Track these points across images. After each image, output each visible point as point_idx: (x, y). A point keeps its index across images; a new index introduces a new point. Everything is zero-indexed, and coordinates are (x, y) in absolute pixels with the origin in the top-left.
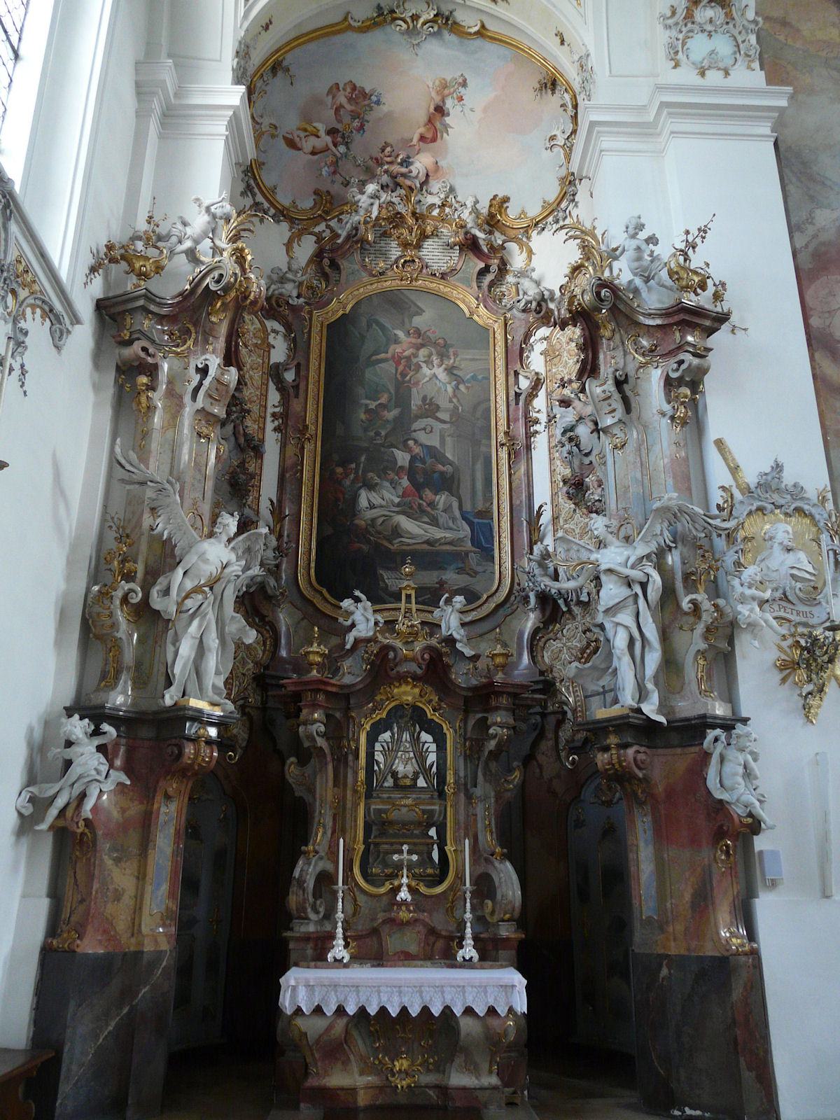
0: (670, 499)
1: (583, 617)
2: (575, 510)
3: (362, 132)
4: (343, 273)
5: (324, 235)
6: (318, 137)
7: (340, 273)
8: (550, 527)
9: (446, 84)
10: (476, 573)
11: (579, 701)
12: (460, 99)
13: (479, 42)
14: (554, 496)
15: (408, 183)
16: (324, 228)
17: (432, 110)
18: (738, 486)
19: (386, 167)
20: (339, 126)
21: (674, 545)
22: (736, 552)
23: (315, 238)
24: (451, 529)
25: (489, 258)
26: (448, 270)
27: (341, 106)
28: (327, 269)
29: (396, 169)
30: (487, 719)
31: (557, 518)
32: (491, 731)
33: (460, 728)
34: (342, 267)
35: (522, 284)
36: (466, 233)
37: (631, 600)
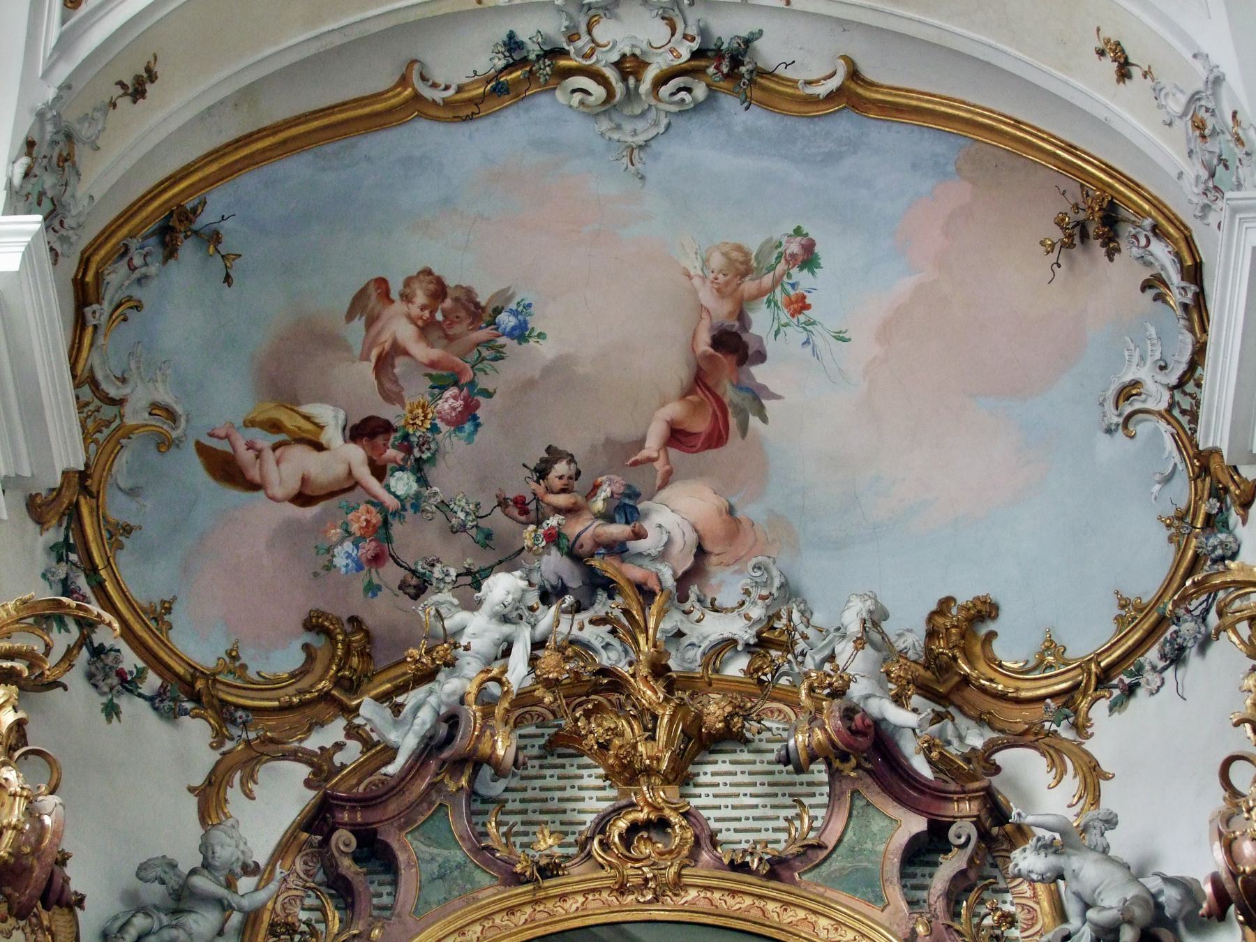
3: (468, 427)
4: (408, 878)
5: (338, 759)
6: (319, 447)
7: (395, 883)
9: (746, 262)
12: (800, 305)
13: (845, 125)
15: (635, 572)
16: (340, 737)
17: (704, 344)
20: (390, 413)
23: (304, 771)
25: (942, 796)
26: (794, 849)
27: (397, 349)
28: (347, 865)
29: (585, 529)
34: (402, 857)
35: (1075, 875)
36: (849, 713)
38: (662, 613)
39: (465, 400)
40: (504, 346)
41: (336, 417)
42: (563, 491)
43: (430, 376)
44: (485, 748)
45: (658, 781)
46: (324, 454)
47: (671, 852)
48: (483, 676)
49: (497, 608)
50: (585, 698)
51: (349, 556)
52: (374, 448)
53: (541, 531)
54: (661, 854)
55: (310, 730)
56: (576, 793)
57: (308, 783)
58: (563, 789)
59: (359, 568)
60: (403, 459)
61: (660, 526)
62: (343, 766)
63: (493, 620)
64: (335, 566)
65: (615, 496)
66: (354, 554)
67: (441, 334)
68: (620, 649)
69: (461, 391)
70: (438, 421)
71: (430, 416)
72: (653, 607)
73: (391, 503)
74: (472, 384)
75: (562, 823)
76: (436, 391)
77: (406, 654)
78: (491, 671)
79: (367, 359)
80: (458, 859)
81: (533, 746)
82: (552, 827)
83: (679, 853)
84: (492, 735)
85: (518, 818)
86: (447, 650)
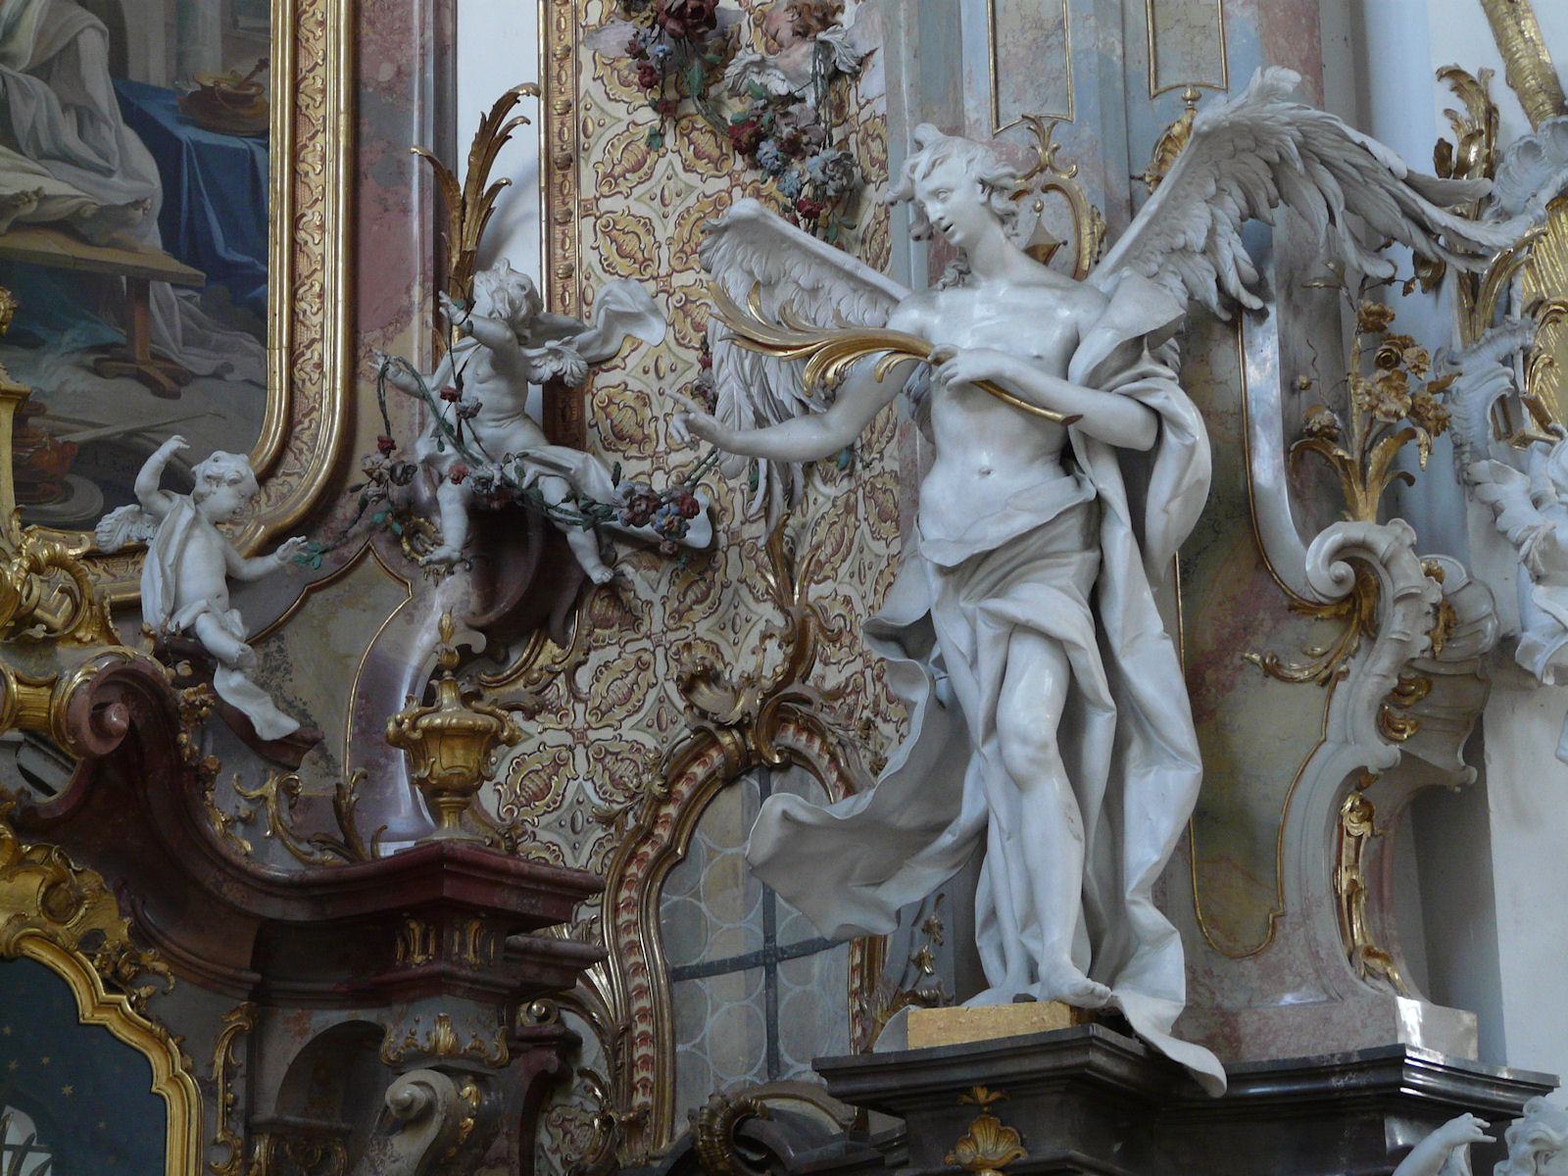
0: (1268, 93)
1: (679, 615)
2: (656, 138)
8: (531, 203)
10: (183, 378)
11: (642, 991)
14: (556, 60)
18: (1513, 80)
21: (1255, 303)
22: (1507, 360)
24: (68, 158)
30: (377, 1033)
31: (569, 162)
32: (404, 1089)
33: (229, 1073)
37: (1072, 530)
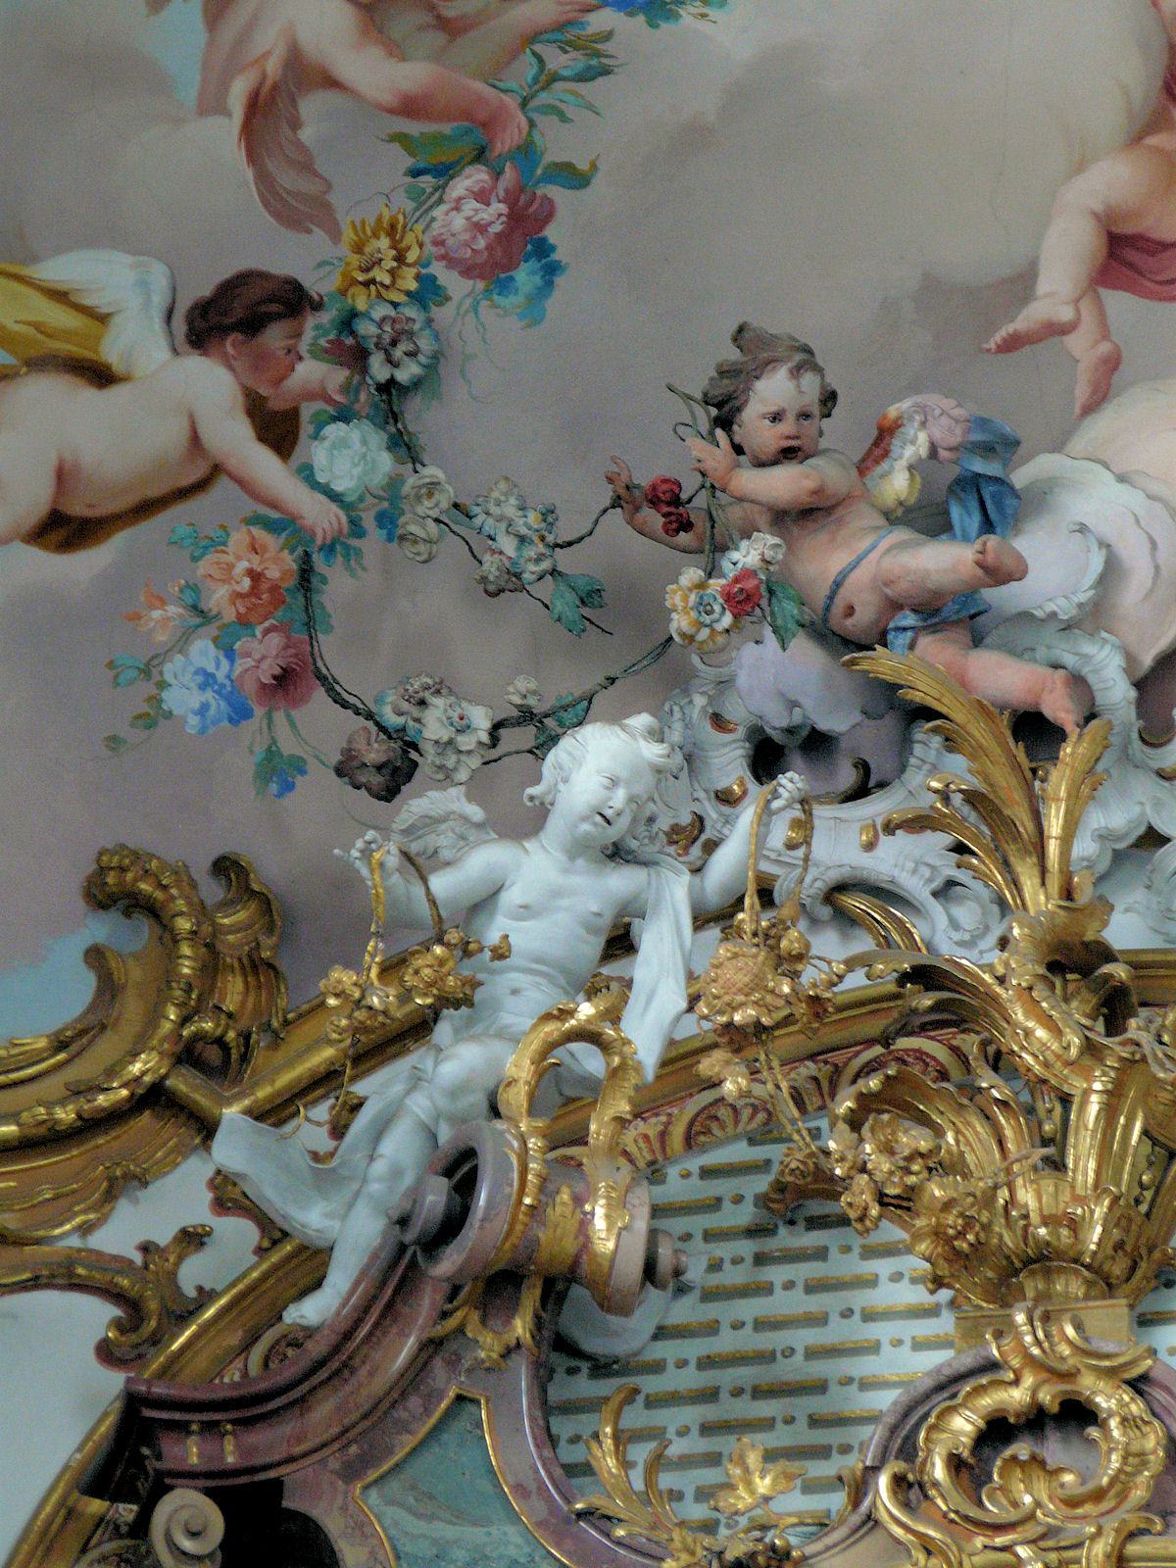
3: (525, 276)
5: (193, 1273)
6: (101, 376)
16: (198, 1210)
19: (746, 555)
23: (97, 1316)
38: (1089, 785)
39: (511, 199)
40: (608, 36)
41: (143, 285)
42: (789, 454)
43: (401, 138)
44: (554, 1240)
45: (1077, 1288)
46: (115, 394)
47: (1098, 1495)
48: (552, 1029)
49: (586, 827)
50: (878, 1050)
51: (207, 680)
52: (260, 361)
53: (716, 584)
54: (1073, 1503)
55: (111, 1196)
56: (857, 1331)
57: (106, 1353)
58: (820, 1320)
59: (240, 713)
60: (345, 388)
61: (1083, 529)
62: (205, 1296)
63: (580, 862)
64: (169, 715)
65: (943, 454)
66: (220, 676)
67: (427, 18)
68: (985, 894)
69: (497, 174)
70: (437, 269)
71: (411, 257)
72: (1055, 775)
73: (320, 516)
74: (526, 151)
75: (815, 1422)
76: (427, 181)
77: (322, 984)
78: (571, 1013)
79: (222, 109)
80: (512, 1551)
81: (738, 1200)
82: (781, 1437)
83: (1123, 1496)
84: (578, 1201)
85: (692, 1415)
86: (442, 962)
